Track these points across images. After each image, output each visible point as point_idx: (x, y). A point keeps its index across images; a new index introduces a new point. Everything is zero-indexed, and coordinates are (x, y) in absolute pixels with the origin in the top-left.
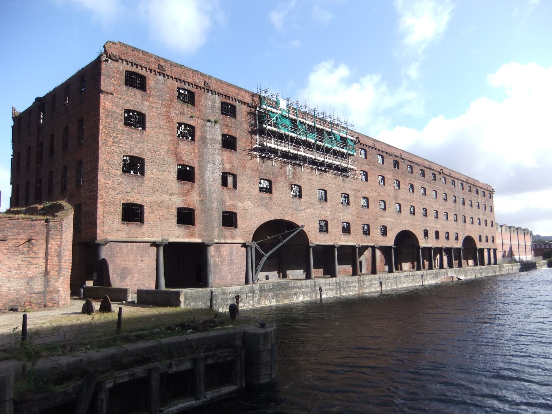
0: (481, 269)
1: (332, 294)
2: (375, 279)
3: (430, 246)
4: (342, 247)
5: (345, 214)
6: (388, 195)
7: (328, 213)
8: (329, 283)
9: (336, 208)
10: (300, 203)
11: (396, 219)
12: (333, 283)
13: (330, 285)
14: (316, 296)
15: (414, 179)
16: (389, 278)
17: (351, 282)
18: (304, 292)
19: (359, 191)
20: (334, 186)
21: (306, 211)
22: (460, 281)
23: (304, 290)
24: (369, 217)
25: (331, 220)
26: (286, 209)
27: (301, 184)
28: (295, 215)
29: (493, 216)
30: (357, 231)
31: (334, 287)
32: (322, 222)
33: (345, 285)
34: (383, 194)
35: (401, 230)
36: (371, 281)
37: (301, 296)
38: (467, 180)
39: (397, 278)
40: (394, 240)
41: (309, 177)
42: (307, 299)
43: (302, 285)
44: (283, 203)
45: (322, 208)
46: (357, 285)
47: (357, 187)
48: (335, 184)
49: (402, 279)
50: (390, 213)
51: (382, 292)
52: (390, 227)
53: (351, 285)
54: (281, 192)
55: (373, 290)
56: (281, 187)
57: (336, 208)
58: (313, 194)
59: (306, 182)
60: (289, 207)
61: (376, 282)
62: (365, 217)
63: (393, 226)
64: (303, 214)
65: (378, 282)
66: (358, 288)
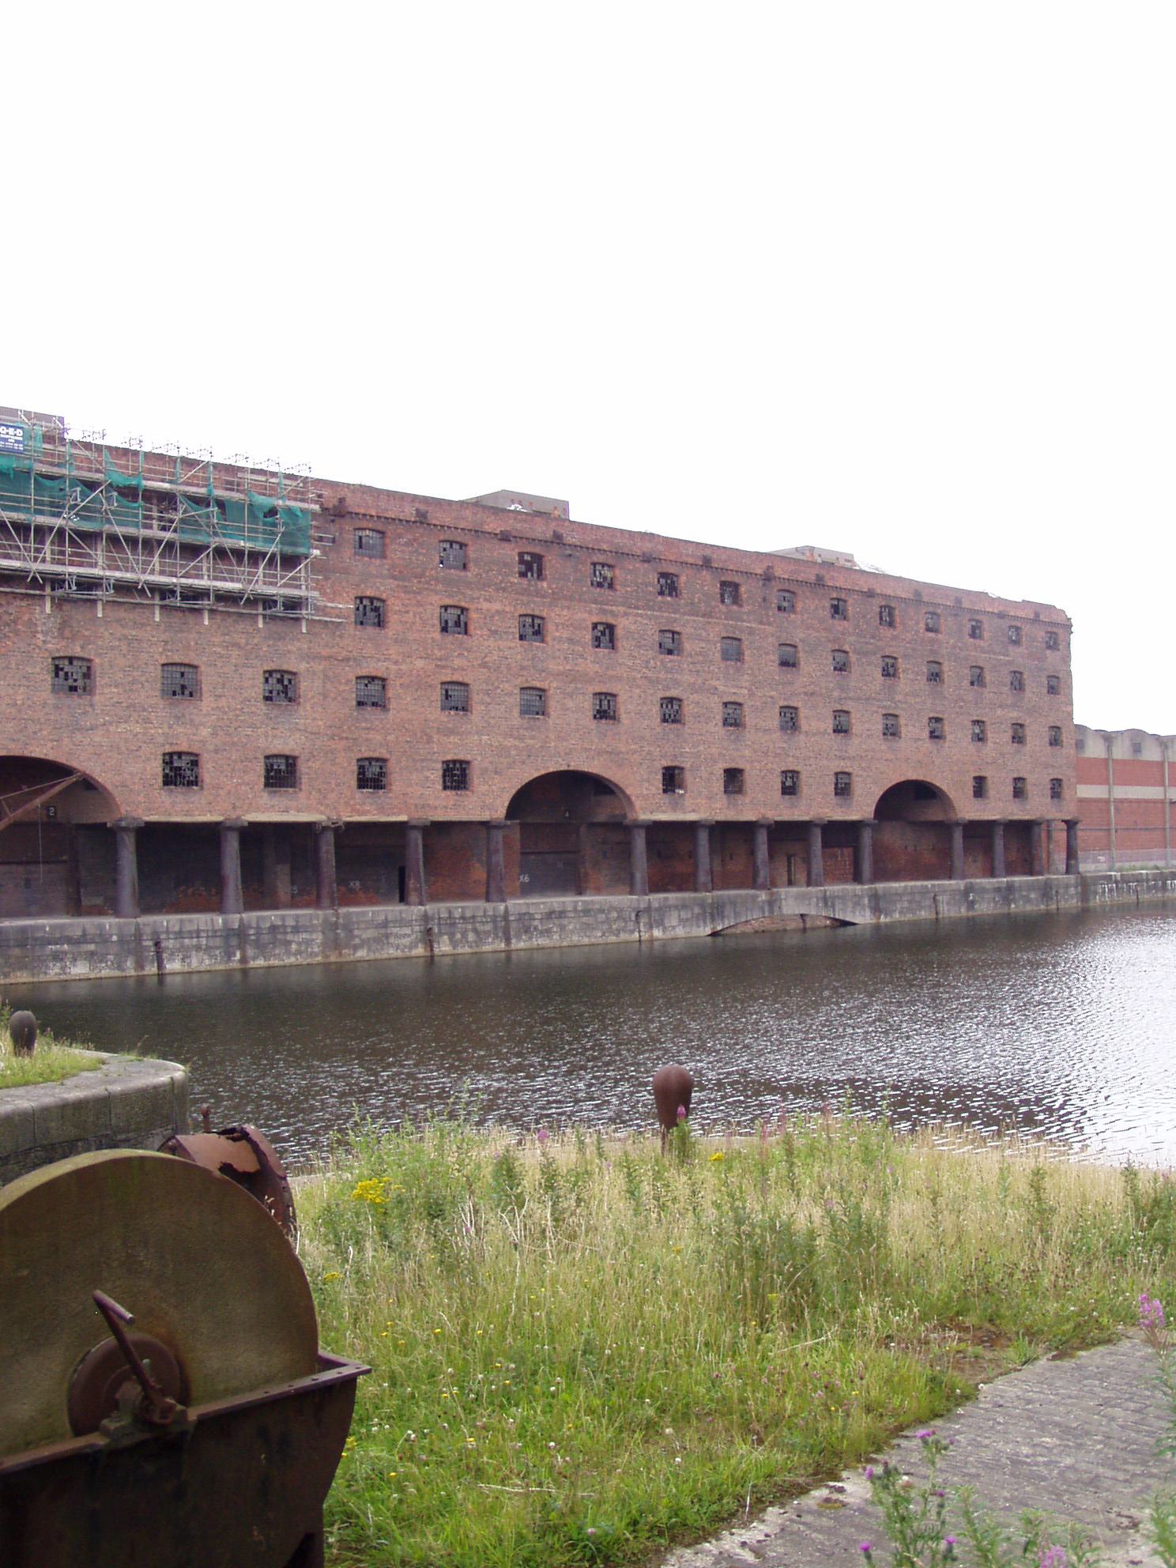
0: (969, 889)
1: (207, 962)
2: (402, 922)
3: (749, 816)
4: (252, 824)
5: (277, 732)
6: (484, 665)
7: (205, 732)
8: (198, 932)
9: (237, 716)
10: (88, 709)
11: (521, 738)
12: (216, 931)
13: (198, 937)
14: (140, 965)
15: (622, 609)
16: (473, 917)
17: (293, 927)
18: (92, 954)
19: (347, 659)
20: (235, 652)
21: (112, 729)
22: (850, 930)
23: (92, 947)
24: (391, 738)
25: (216, 751)
26: (32, 728)
27: (93, 652)
28: (66, 741)
29: (1069, 709)
30: (333, 782)
31: (218, 942)
32: (180, 757)
33: (266, 938)
34: (457, 662)
35: (543, 772)
36: (385, 924)
37: (78, 963)
38: (918, 594)
39: (512, 918)
40: (506, 804)
41: (125, 632)
42: (105, 973)
43: (84, 934)
44: (20, 711)
45: (177, 718)
46: (320, 936)
47: (334, 650)
48: (237, 645)
49: (536, 923)
50: (492, 722)
51: (431, 960)
52: (491, 763)
53: (289, 937)
54: (12, 682)
55: (392, 952)
56: (13, 666)
57: (237, 716)
58: (143, 679)
59: (113, 648)
60: (42, 720)
61: (407, 931)
62: (371, 736)
63: (505, 761)
64: (97, 739)
65: (417, 928)
66: (324, 944)
